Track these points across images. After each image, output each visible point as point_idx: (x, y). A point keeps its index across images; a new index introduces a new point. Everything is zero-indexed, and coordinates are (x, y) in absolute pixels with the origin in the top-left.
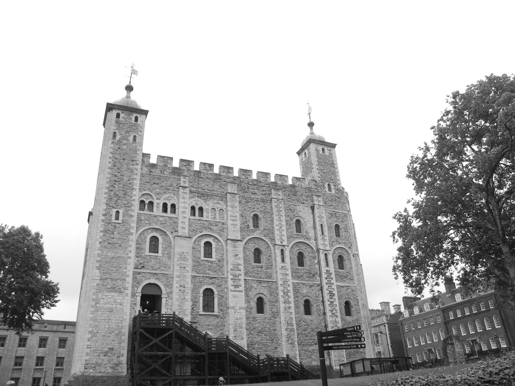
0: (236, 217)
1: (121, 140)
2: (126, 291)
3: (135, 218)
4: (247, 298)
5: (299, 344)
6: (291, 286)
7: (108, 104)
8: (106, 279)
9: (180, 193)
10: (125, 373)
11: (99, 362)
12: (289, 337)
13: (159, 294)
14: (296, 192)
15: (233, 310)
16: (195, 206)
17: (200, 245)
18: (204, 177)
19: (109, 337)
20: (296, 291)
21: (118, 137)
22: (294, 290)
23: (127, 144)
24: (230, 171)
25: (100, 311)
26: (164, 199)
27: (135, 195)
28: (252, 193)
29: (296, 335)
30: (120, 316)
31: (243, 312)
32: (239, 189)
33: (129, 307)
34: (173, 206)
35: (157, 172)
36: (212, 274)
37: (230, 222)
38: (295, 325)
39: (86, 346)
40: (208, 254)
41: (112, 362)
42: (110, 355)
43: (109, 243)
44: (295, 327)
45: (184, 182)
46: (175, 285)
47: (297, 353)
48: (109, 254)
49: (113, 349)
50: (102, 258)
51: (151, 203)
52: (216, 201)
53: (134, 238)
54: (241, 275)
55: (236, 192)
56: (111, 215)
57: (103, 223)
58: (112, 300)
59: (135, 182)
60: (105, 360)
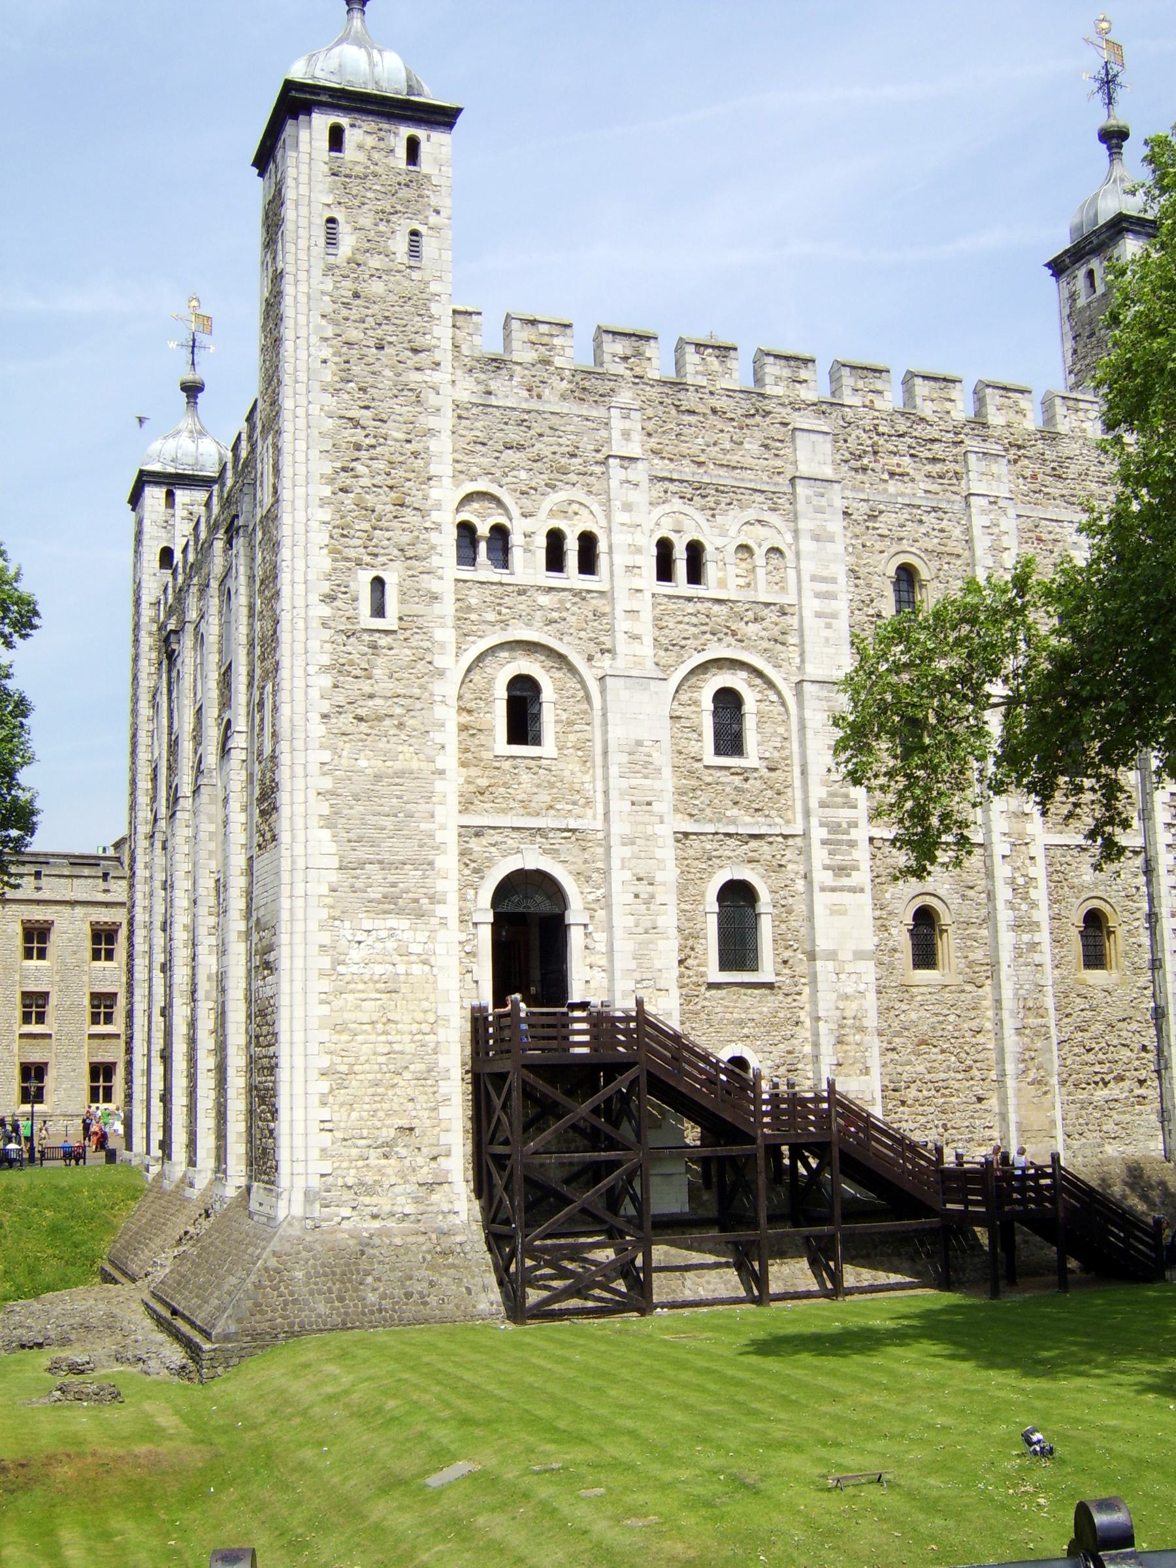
0: (834, 581)
1: (360, 258)
2: (440, 910)
3: (447, 607)
4: (878, 913)
5: (1063, 1083)
6: (1041, 861)
7: (289, 85)
8: (362, 864)
9: (614, 483)
10: (464, 1216)
11: (369, 1180)
12: (1027, 1058)
13: (557, 911)
14: (1062, 462)
15: (830, 965)
16: (673, 537)
17: (696, 703)
18: (701, 408)
19: (393, 1086)
20: (1058, 877)
21: (348, 242)
22: (1049, 875)
23: (388, 272)
24: (803, 374)
25: (352, 992)
26: (552, 514)
27: (438, 506)
28: (892, 474)
29: (1055, 1047)
30: (425, 1005)
31: (869, 971)
32: (838, 457)
33: (455, 969)
34: (588, 542)
35: (509, 393)
36: (748, 824)
37: (811, 605)
38: (1052, 1012)
39: (317, 1126)
40: (729, 740)
41: (414, 1179)
42: (403, 1152)
43: (360, 719)
44: (1052, 1024)
45: (626, 435)
46: (619, 876)
47: (1058, 1114)
48: (363, 763)
49: (411, 1129)
50: (338, 780)
51: (500, 534)
52: (751, 514)
53: (448, 687)
54: (856, 826)
55: (828, 472)
56: (355, 600)
57: (327, 634)
58: (391, 945)
59: (433, 444)
60: (389, 1171)
